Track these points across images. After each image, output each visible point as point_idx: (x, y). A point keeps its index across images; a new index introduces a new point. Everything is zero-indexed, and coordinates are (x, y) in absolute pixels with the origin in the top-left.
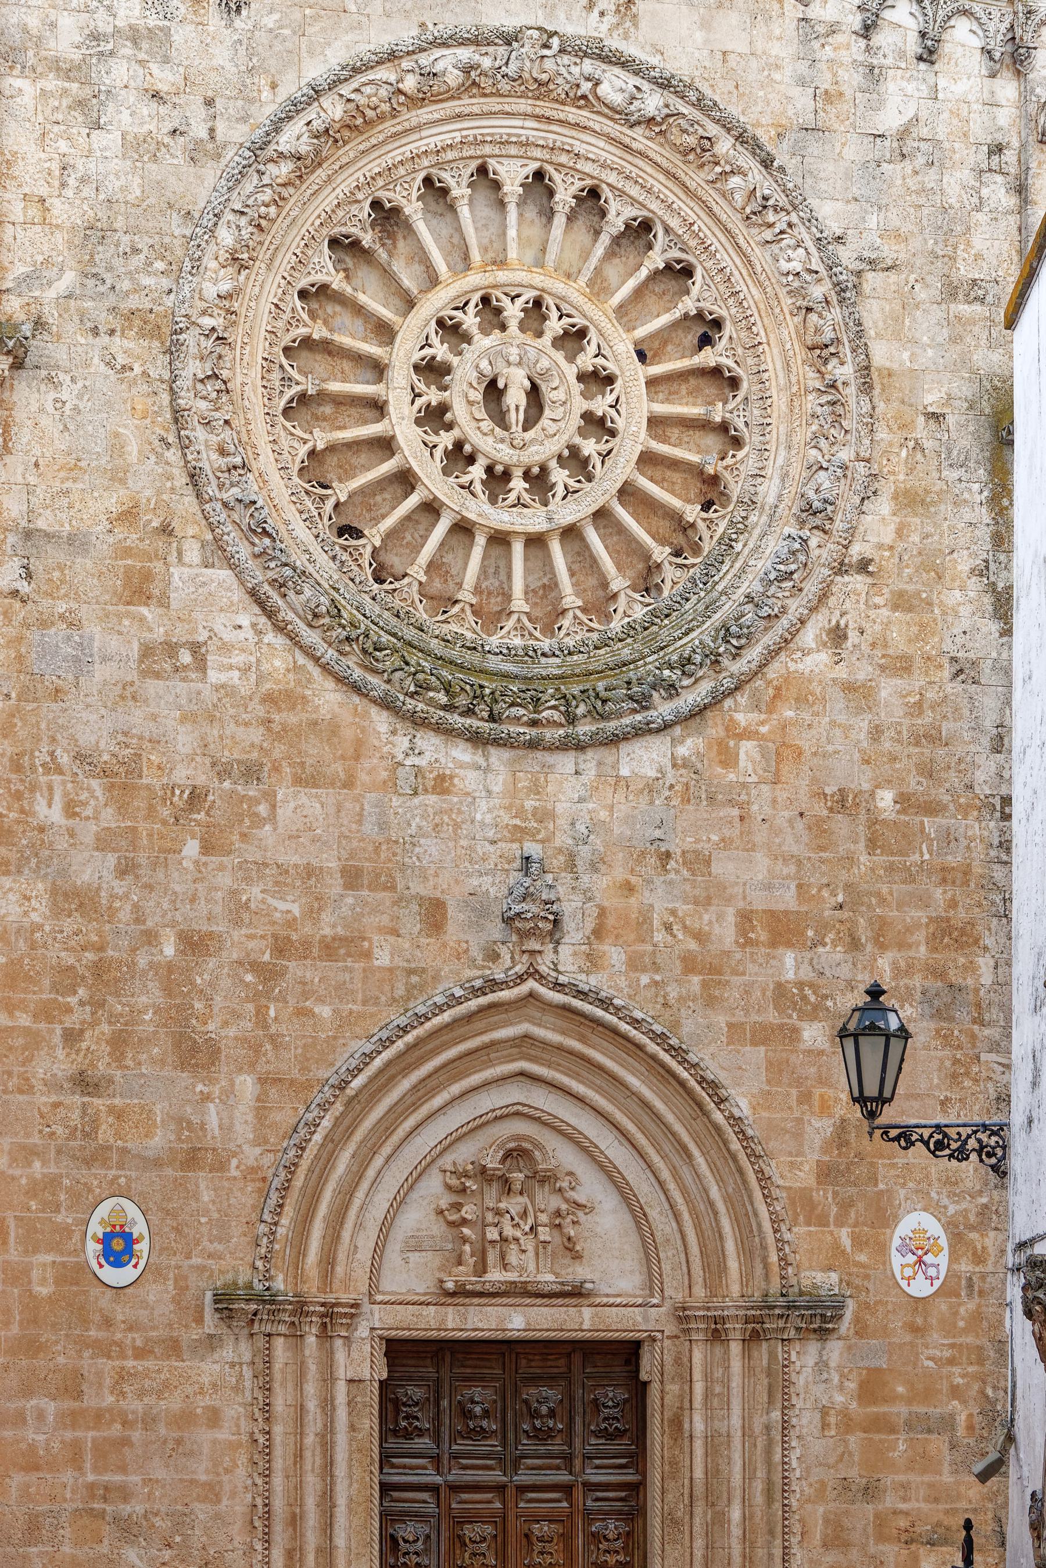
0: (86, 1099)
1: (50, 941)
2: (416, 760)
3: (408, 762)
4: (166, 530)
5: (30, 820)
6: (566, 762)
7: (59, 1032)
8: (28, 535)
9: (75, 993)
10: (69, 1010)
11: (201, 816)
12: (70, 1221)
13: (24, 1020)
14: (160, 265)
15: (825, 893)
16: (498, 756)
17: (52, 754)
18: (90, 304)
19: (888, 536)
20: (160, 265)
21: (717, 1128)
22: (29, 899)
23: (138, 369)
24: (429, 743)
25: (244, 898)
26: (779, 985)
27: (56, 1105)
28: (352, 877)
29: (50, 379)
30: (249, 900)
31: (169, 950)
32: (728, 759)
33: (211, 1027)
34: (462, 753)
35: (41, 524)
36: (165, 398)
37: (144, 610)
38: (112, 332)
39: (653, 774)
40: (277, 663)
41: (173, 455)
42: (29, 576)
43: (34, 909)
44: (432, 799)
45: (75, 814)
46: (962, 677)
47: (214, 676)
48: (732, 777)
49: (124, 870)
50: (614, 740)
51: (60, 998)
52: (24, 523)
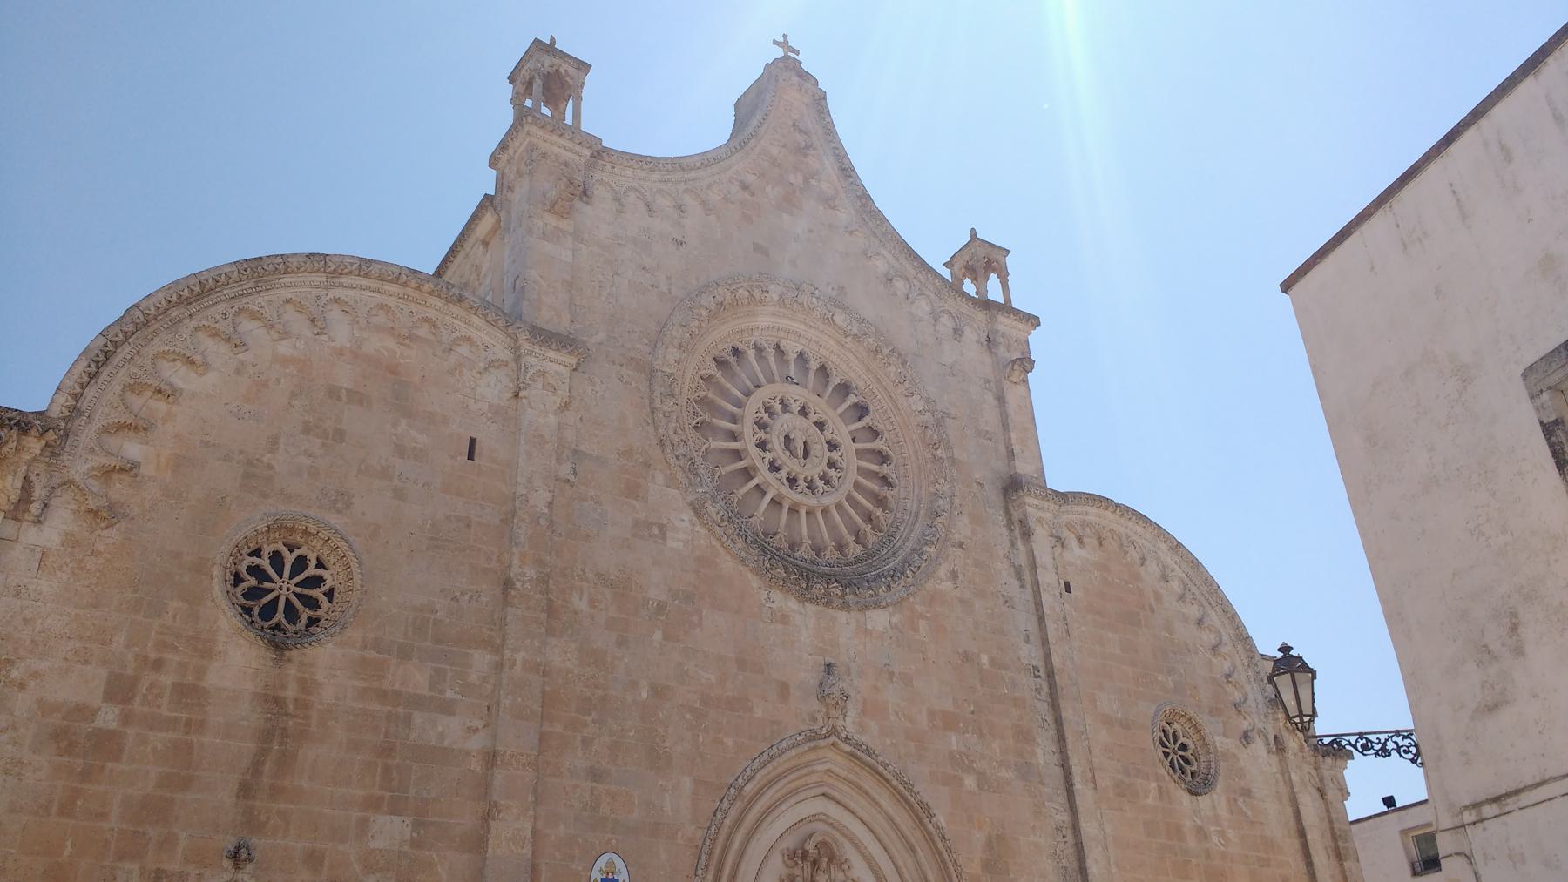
0: (594, 784)
1: (577, 680)
2: (772, 605)
3: (767, 605)
4: (647, 465)
5: (569, 605)
6: (842, 616)
7: (579, 738)
8: (576, 452)
9: (590, 714)
10: (586, 725)
11: (663, 618)
12: (580, 868)
13: (558, 728)
14: (645, 341)
15: (966, 705)
16: (811, 608)
17: (583, 570)
18: (611, 350)
19: (969, 533)
20: (645, 341)
21: (929, 834)
22: (566, 653)
23: (634, 385)
24: (777, 596)
25: (686, 668)
26: (951, 753)
27: (576, 787)
28: (742, 664)
29: (589, 379)
30: (688, 669)
31: (645, 695)
32: (915, 629)
33: (667, 744)
34: (792, 604)
35: (582, 448)
36: (647, 401)
37: (635, 502)
38: (622, 365)
39: (881, 629)
40: (702, 542)
41: (650, 428)
42: (575, 473)
43: (569, 660)
44: (780, 626)
45: (594, 607)
46: (1007, 605)
47: (671, 543)
48: (917, 637)
49: (622, 642)
50: (866, 608)
51: (581, 717)
52: (573, 446)
